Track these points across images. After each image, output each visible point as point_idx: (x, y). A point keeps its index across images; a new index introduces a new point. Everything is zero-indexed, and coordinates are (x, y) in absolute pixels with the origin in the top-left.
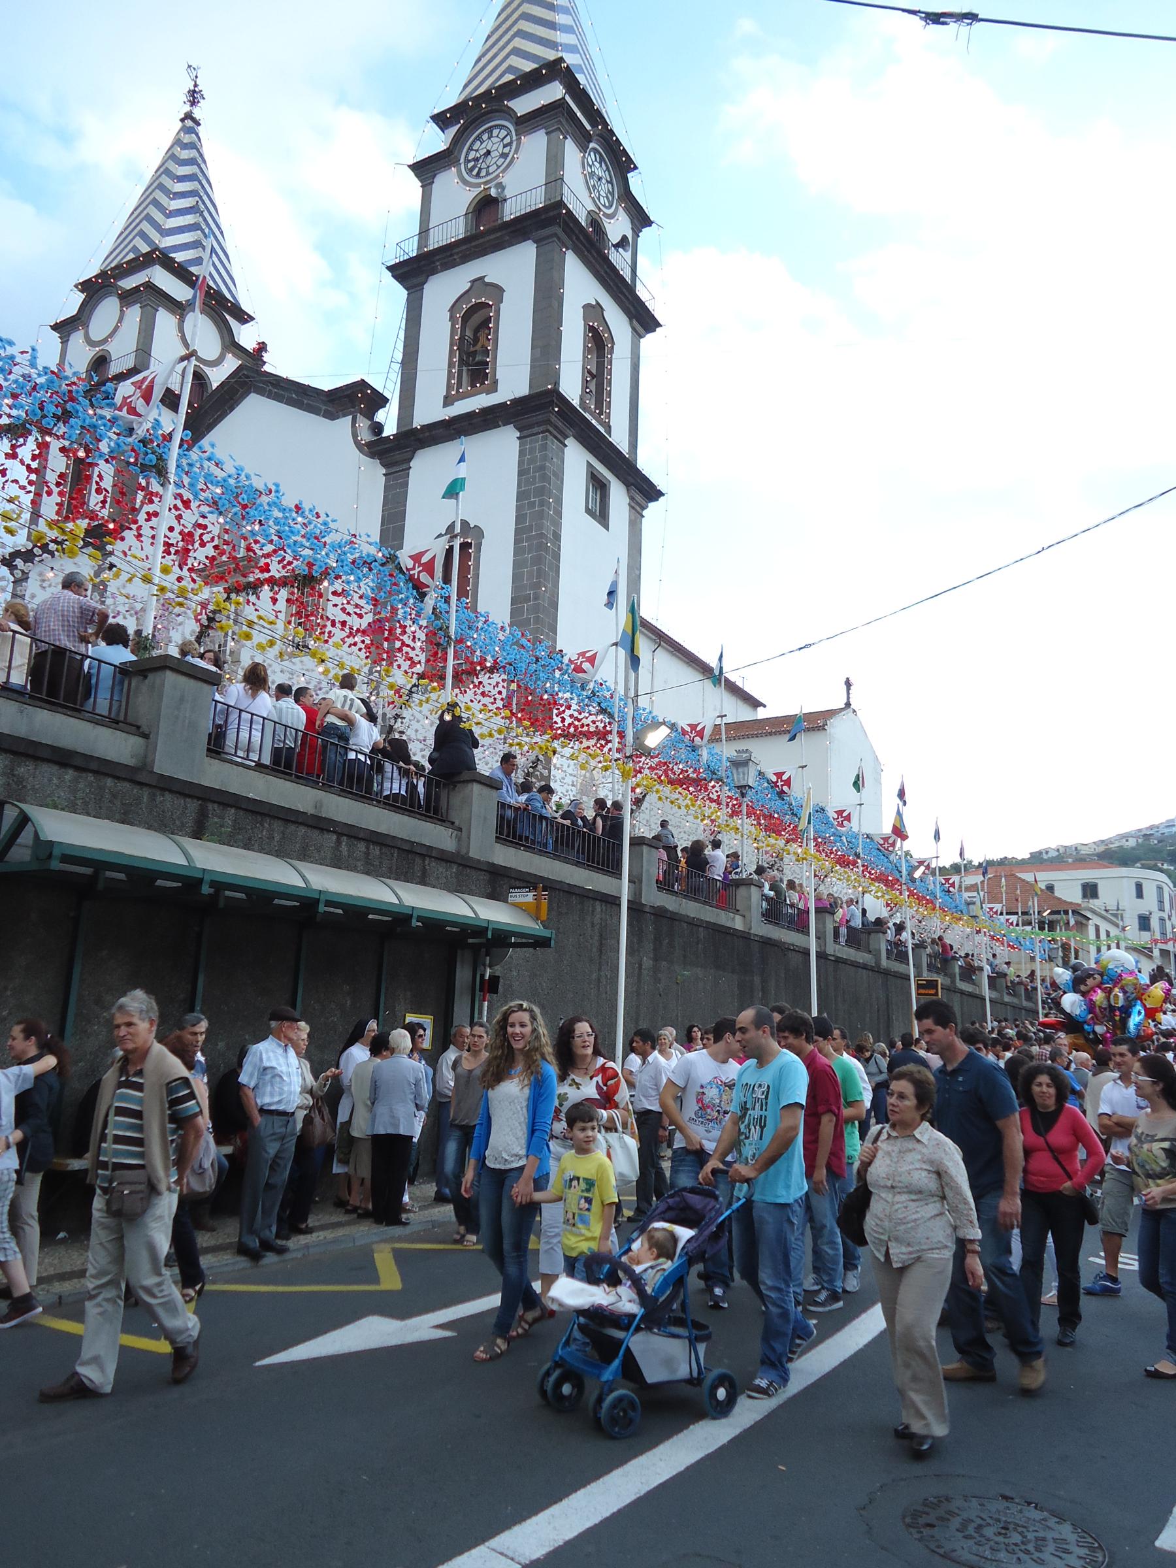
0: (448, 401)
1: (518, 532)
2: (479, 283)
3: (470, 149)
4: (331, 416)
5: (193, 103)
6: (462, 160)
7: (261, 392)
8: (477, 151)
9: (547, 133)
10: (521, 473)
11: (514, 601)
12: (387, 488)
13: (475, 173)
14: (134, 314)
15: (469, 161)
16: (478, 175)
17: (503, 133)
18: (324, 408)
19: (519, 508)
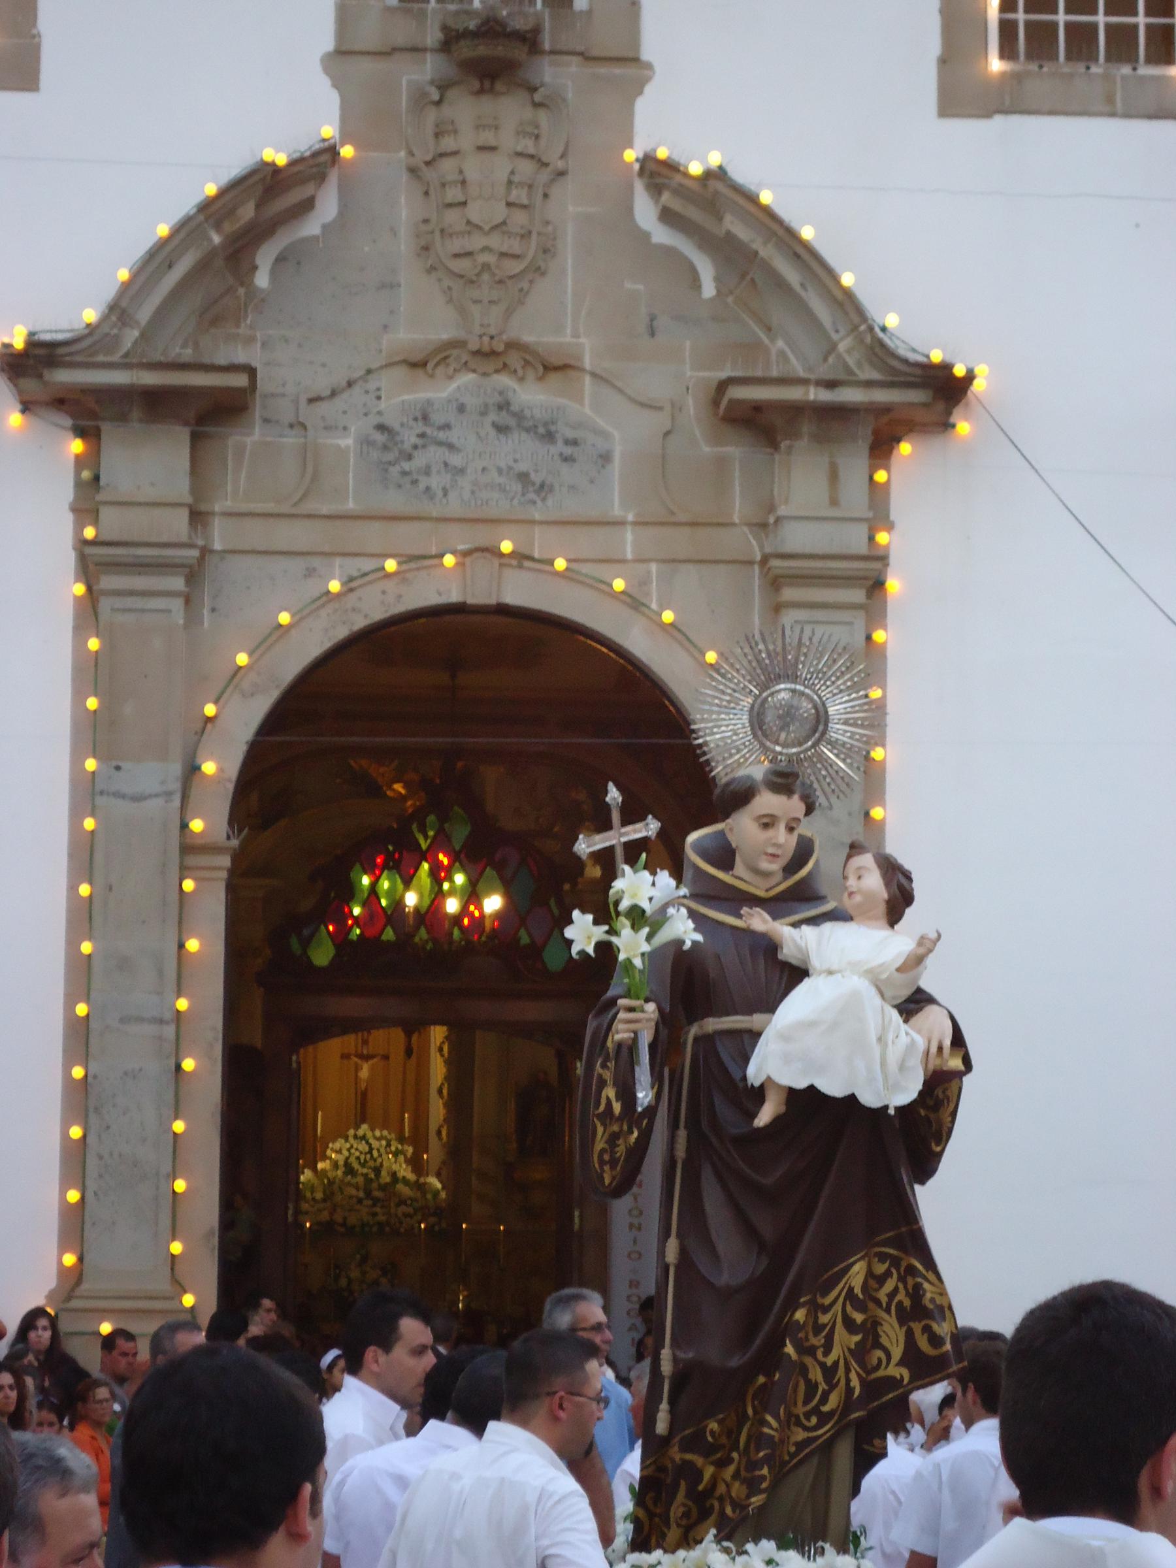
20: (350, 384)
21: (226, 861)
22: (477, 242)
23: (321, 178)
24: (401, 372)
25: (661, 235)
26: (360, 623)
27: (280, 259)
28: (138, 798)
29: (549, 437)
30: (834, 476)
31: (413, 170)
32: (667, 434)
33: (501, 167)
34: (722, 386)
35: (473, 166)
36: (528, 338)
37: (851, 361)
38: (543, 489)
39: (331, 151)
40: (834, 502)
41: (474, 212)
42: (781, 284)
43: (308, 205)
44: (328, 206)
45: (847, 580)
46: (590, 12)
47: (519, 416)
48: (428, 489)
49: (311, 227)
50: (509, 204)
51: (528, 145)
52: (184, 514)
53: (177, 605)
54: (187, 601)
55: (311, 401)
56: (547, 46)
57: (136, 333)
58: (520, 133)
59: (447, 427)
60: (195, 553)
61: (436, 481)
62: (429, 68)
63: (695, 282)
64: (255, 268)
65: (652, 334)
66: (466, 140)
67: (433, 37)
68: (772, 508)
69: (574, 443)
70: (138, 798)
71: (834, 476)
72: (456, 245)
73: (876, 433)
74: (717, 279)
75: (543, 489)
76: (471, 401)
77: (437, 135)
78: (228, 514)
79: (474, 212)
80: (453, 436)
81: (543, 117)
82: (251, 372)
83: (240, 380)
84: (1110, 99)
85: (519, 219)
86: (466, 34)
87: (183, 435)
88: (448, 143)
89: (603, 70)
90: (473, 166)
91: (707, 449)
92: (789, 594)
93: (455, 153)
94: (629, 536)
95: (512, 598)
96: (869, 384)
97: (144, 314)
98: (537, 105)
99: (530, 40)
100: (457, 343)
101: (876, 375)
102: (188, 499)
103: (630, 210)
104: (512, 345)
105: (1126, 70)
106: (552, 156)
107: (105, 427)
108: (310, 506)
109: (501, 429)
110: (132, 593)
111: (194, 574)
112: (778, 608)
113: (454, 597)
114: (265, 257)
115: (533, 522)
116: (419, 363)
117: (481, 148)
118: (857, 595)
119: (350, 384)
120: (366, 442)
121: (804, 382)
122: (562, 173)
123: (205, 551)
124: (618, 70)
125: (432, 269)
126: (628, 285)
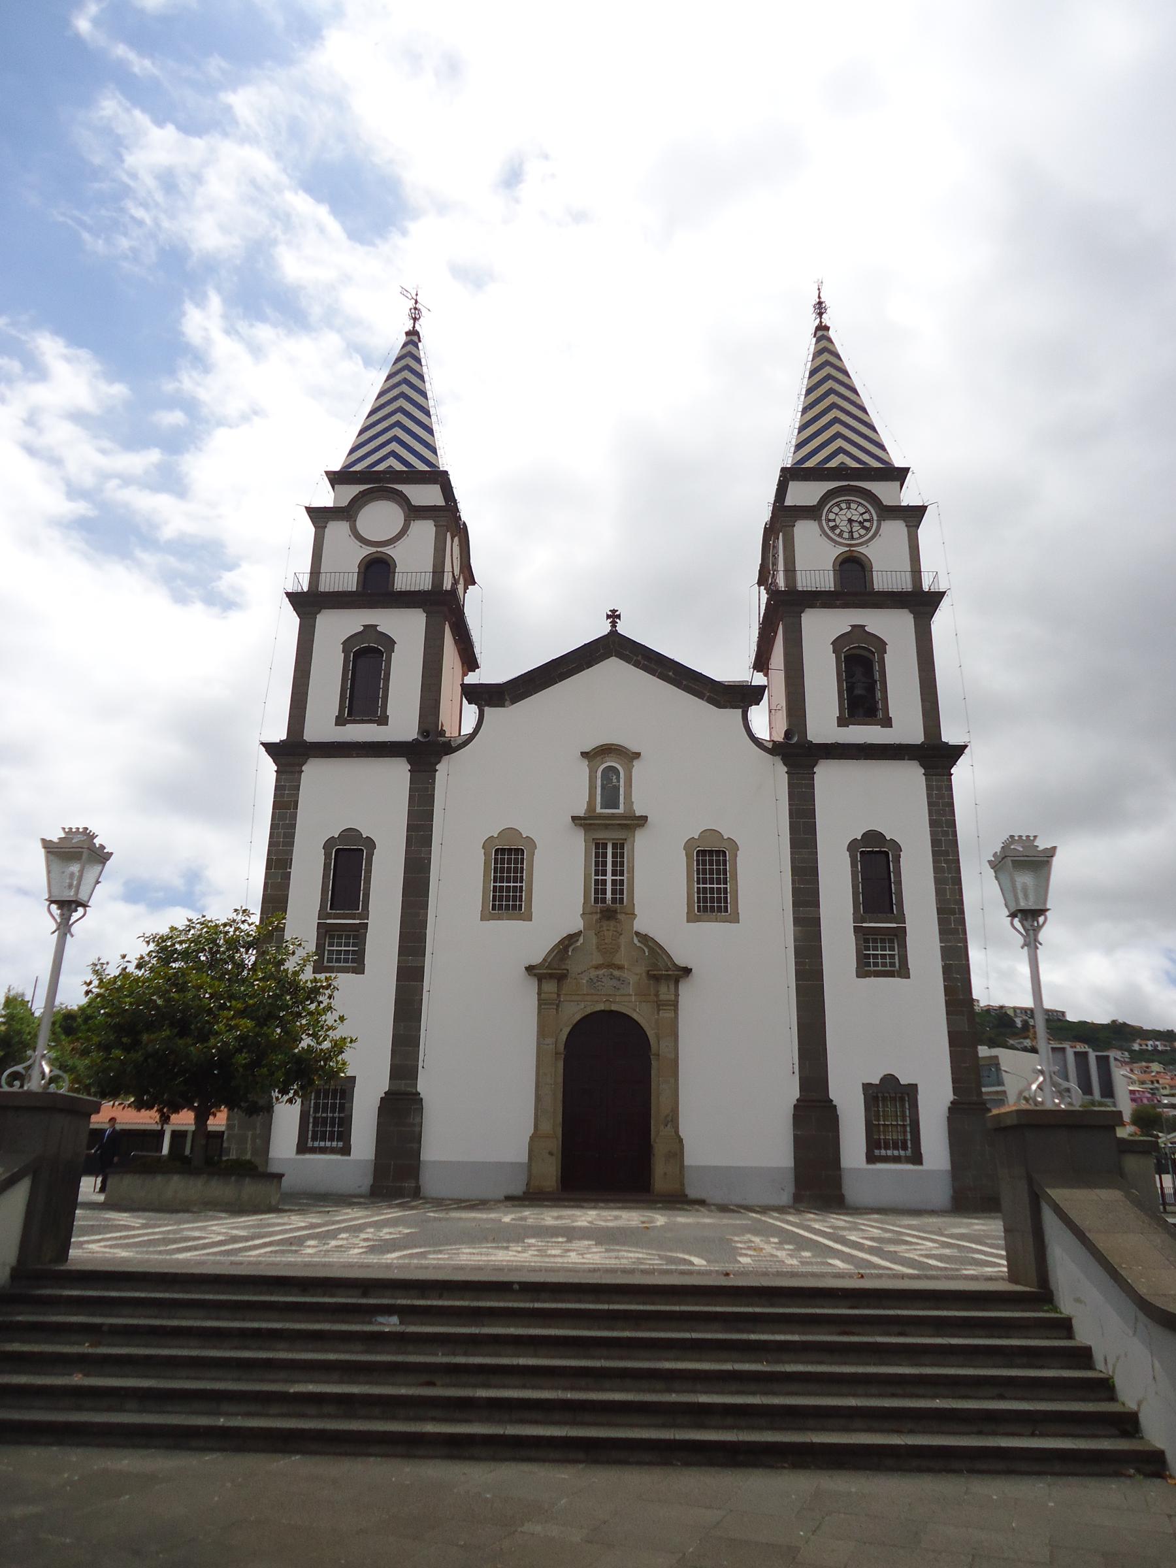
0: (842, 722)
1: (934, 853)
2: (858, 630)
3: (830, 511)
4: (719, 705)
5: (415, 319)
6: (824, 518)
7: (627, 660)
8: (837, 514)
9: (906, 526)
10: (930, 804)
11: (940, 911)
12: (791, 786)
13: (838, 531)
14: (425, 531)
15: (830, 520)
16: (840, 535)
17: (861, 510)
18: (708, 694)
19: (932, 834)
20: (585, 971)
21: (563, 1056)
22: (607, 946)
23: (580, 935)
24: (593, 969)
25: (639, 944)
26: (586, 1014)
27: (573, 950)
28: (548, 1045)
29: (619, 980)
30: (668, 986)
31: (596, 934)
32: (639, 979)
33: (611, 933)
34: (649, 971)
35: (606, 933)
36: (616, 963)
37: (670, 967)
38: (618, 989)
39: (581, 931)
40: (669, 991)
41: (606, 941)
42: (658, 953)
43: (578, 940)
44: (581, 940)
45: (671, 1005)
46: (626, 906)
47: (614, 976)
48: (598, 990)
49: (578, 944)
50: (612, 940)
51: (615, 929)
52: (556, 995)
53: (555, 1010)
54: (557, 1010)
55: (579, 974)
56: (619, 911)
57: (547, 964)
58: (614, 927)
59: (601, 978)
60: (557, 1002)
61: (600, 988)
62: (599, 916)
63: (644, 951)
64: (568, 951)
65: (637, 962)
66: (605, 928)
67: (599, 911)
68: (658, 992)
69: (623, 981)
70: (548, 1045)
71: (668, 986)
72: (603, 947)
73: (676, 979)
74: (648, 952)
75: (618, 989)
76: (606, 974)
77: (600, 928)
78: (565, 994)
79: (606, 941)
80: (603, 980)
81: (618, 924)
82: (568, 970)
83: (565, 971)
84: (717, 919)
85: (614, 942)
86: (604, 911)
87: (556, 981)
88: (602, 929)
89: (628, 916)
90: (606, 933)
91: (646, 981)
92: (661, 1008)
93: (603, 931)
94: (633, 997)
95: (612, 1009)
96: (673, 971)
97: (549, 960)
98: (617, 922)
99: (615, 912)
100: (603, 964)
101: (674, 969)
102: (556, 991)
103: (633, 941)
104: (614, 964)
105: (719, 914)
106: (620, 931)
107: (543, 980)
108: (578, 993)
109: (611, 979)
110: (547, 1009)
111: (558, 1006)
112: (659, 1010)
113: (603, 1008)
114: (570, 950)
115: (616, 995)
116: (597, 967)
117: (608, 930)
118: (673, 1008)
119: (585, 971)
120: (587, 981)
121: (662, 971)
122: (621, 934)
123: (560, 1001)
124: (631, 916)
125: (599, 951)
126: (633, 953)
